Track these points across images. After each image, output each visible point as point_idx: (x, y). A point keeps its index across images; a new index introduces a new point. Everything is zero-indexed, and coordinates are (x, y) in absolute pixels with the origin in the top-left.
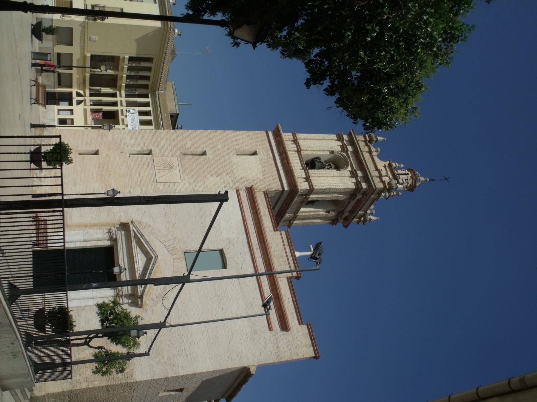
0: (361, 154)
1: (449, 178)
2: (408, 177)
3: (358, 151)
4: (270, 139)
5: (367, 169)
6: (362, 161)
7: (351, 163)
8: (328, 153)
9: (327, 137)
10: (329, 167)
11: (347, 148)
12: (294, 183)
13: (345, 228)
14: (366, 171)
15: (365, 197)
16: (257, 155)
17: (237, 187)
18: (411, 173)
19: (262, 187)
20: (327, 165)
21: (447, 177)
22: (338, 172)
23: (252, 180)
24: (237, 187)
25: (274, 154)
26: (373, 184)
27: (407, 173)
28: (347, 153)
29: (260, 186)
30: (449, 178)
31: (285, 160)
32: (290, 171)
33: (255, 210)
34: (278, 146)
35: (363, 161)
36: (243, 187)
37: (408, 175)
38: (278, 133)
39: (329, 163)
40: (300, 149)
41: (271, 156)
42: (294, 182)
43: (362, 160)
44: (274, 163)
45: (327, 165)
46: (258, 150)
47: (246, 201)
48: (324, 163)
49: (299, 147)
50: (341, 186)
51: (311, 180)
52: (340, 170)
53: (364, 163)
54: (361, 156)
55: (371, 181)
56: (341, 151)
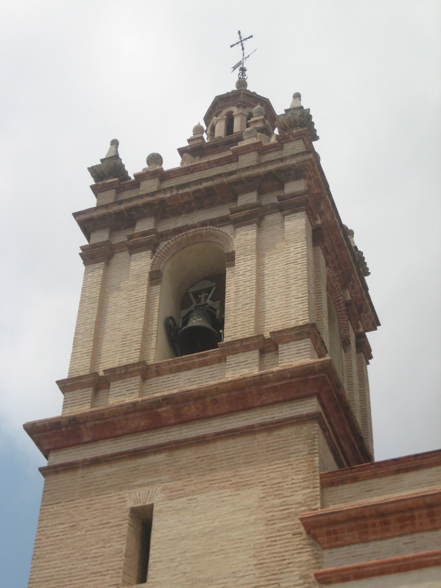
0: (175, 192)
1: (239, 32)
2: (241, 114)
3: (162, 202)
4: (85, 460)
5: (234, 177)
6: (199, 190)
7: (203, 224)
8: (157, 289)
9: (94, 290)
10: (206, 298)
11: (144, 234)
12: (294, 380)
13: (378, 327)
14: (239, 182)
15: (323, 207)
16: (152, 506)
17: (301, 582)
18: (229, 106)
19: (304, 488)
20: (205, 301)
21: (238, 40)
22: (239, 258)
23: (267, 525)
24: (301, 582)
25: (152, 447)
26: (294, 161)
27: (225, 117)
28: (163, 236)
29: (299, 497)
30: (239, 32)
31: (186, 408)
32: (235, 393)
33: (416, 513)
34: (118, 432)
35: (201, 187)
36: (303, 559)
37: (234, 114)
38: (64, 429)
39: (191, 295)
40: (138, 364)
41: (161, 457)
42: (286, 378)
43: (194, 192)
44: (194, 449)
45: (205, 301)
46: (130, 504)
47: (371, 547)
48: (192, 307)
49: (126, 367)
50: (299, 250)
51: (272, 333)
52: (233, 253)
53: (209, 184)
54: (181, 192)
55: (281, 165)
56: (154, 252)
